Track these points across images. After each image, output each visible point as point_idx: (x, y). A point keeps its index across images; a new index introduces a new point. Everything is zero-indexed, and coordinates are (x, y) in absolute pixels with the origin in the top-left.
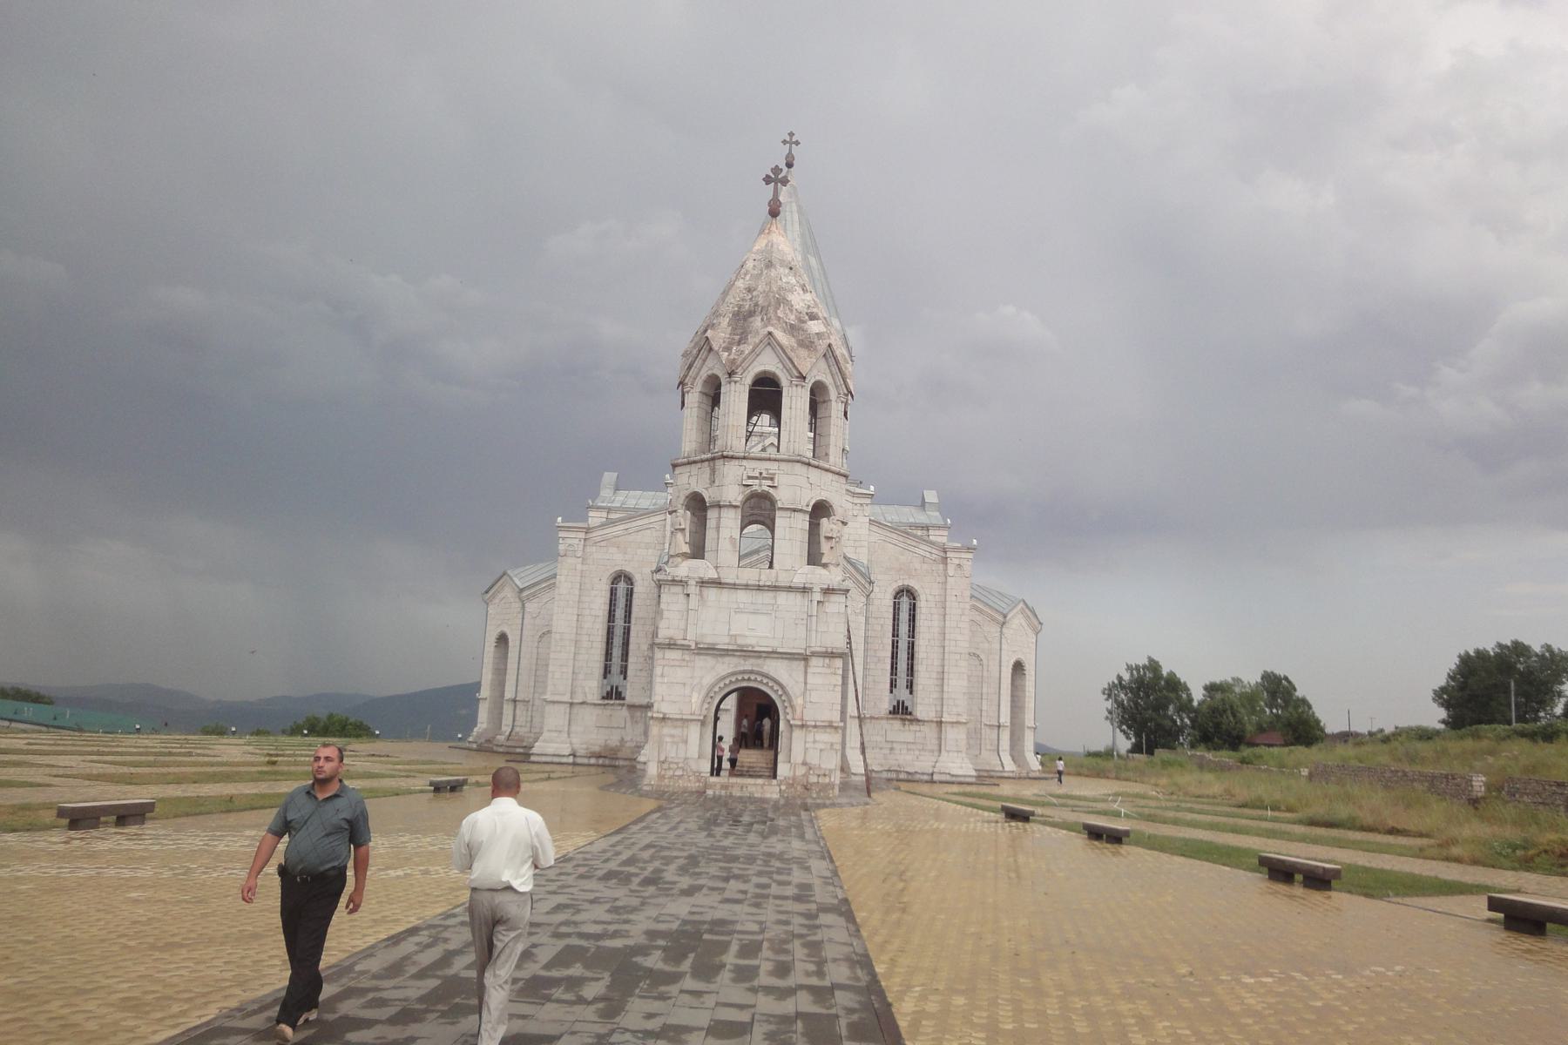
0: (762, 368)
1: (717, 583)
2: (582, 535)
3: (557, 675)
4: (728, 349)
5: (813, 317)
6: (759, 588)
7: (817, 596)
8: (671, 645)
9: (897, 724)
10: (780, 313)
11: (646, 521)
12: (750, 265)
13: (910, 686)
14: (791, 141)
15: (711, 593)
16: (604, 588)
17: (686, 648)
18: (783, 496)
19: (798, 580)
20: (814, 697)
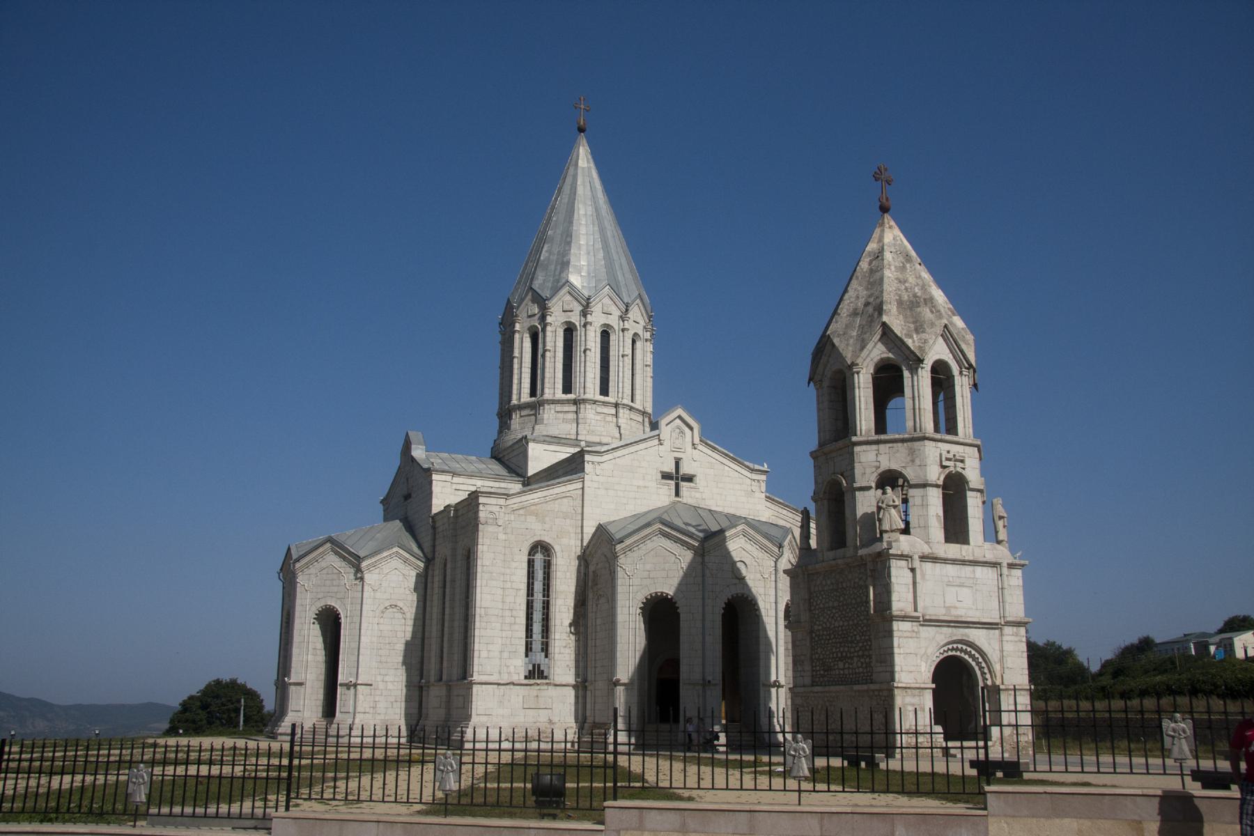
0: (937, 357)
2: (502, 502)
3: (484, 654)
4: (911, 337)
6: (963, 562)
7: (1005, 571)
8: (905, 618)
11: (563, 489)
12: (888, 256)
15: (928, 566)
16: (525, 559)
19: (990, 557)
20: (1009, 662)
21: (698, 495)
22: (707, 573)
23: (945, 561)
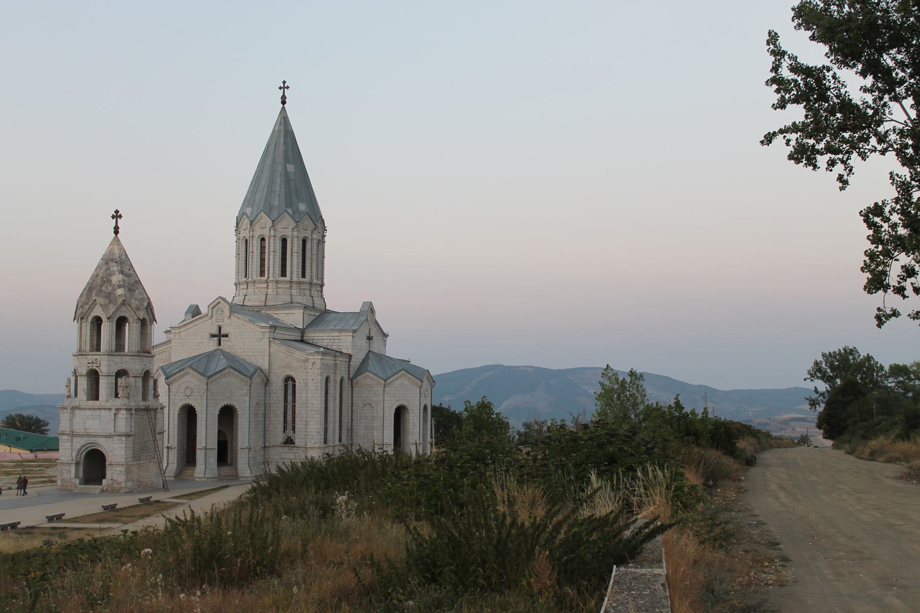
1: (78, 408)
5: (120, 287)
7: (113, 412)
9: (286, 449)
10: (103, 288)
13: (294, 428)
14: (284, 87)
15: (77, 412)
17: (68, 435)
18: (103, 369)
19: (108, 405)
20: (115, 453)
21: (230, 344)
22: (171, 394)
23: (85, 409)
